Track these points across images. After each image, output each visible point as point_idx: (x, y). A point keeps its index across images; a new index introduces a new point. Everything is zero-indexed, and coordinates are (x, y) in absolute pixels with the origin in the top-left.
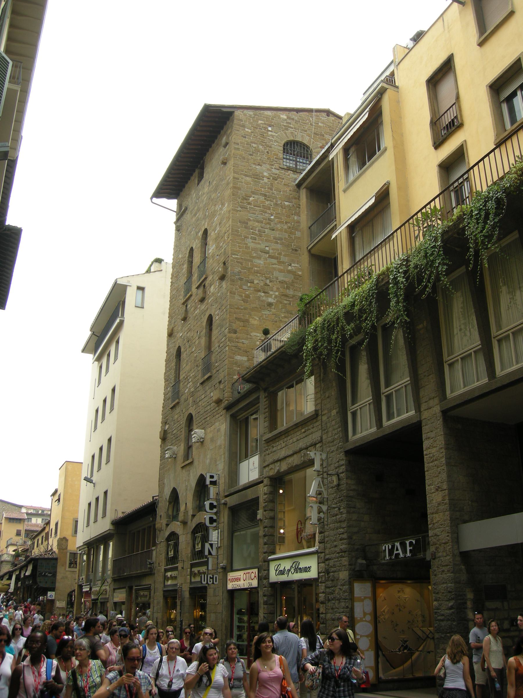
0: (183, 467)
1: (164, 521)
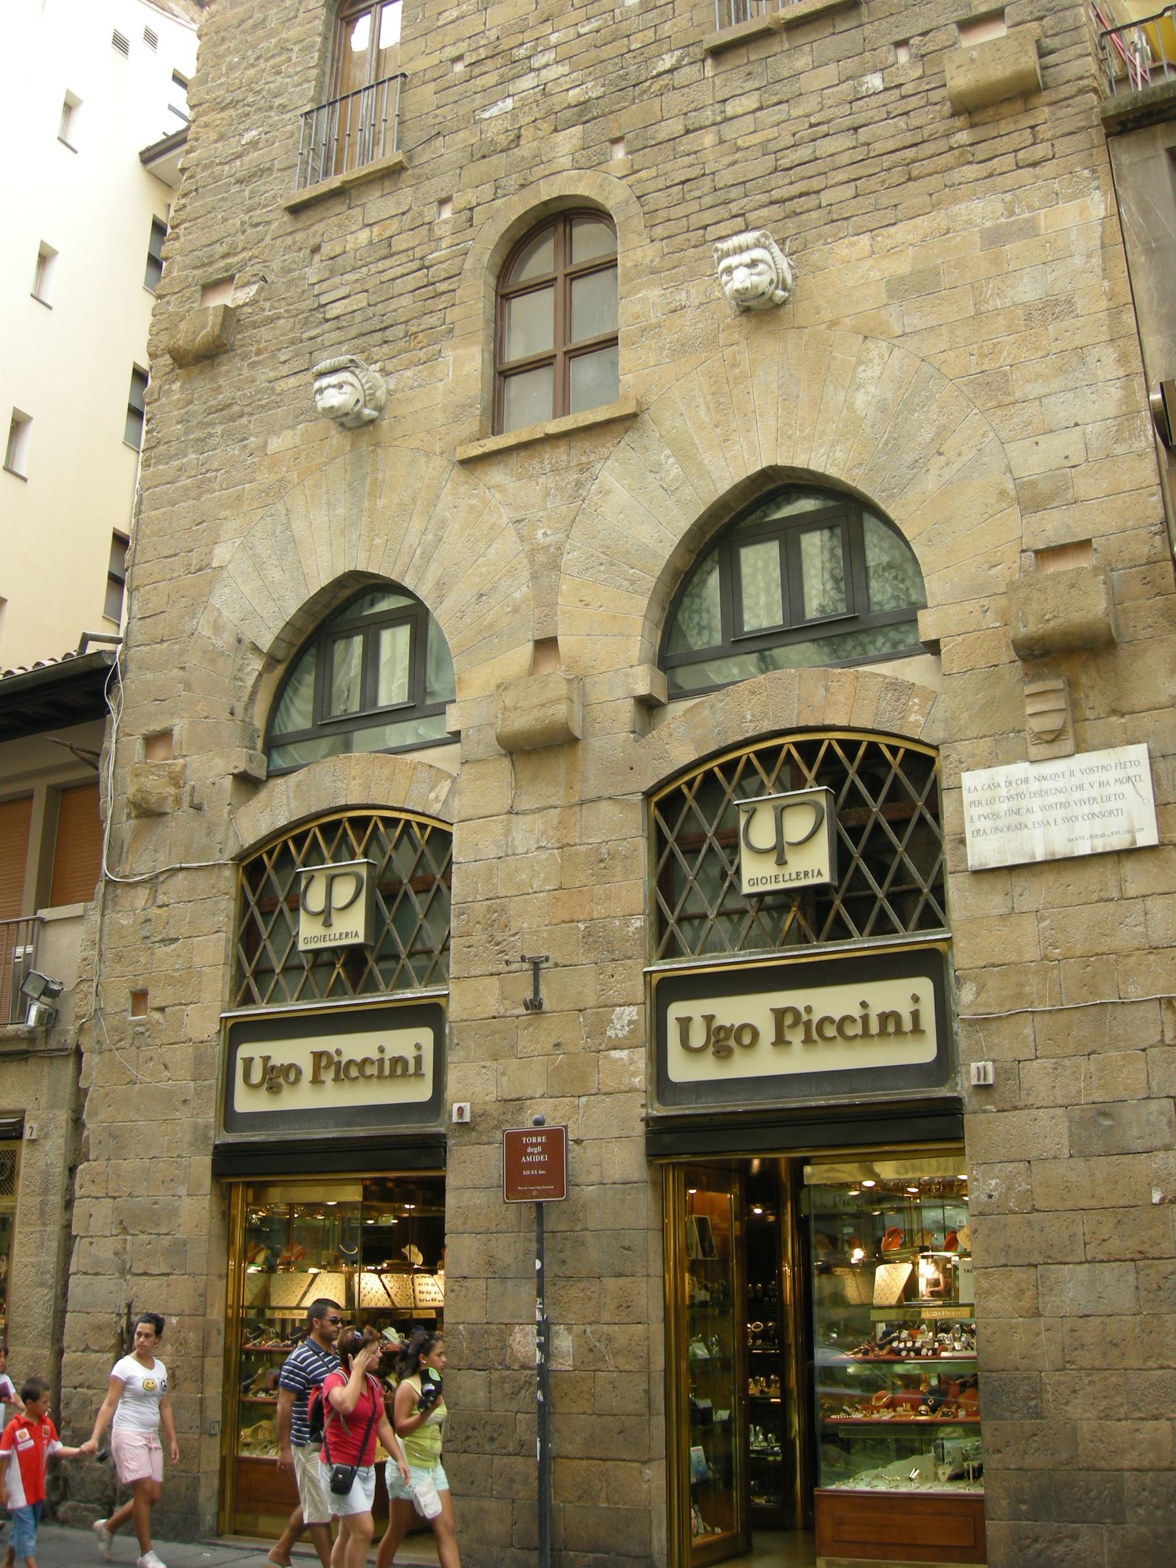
0: (469, 463)
1: (213, 766)
